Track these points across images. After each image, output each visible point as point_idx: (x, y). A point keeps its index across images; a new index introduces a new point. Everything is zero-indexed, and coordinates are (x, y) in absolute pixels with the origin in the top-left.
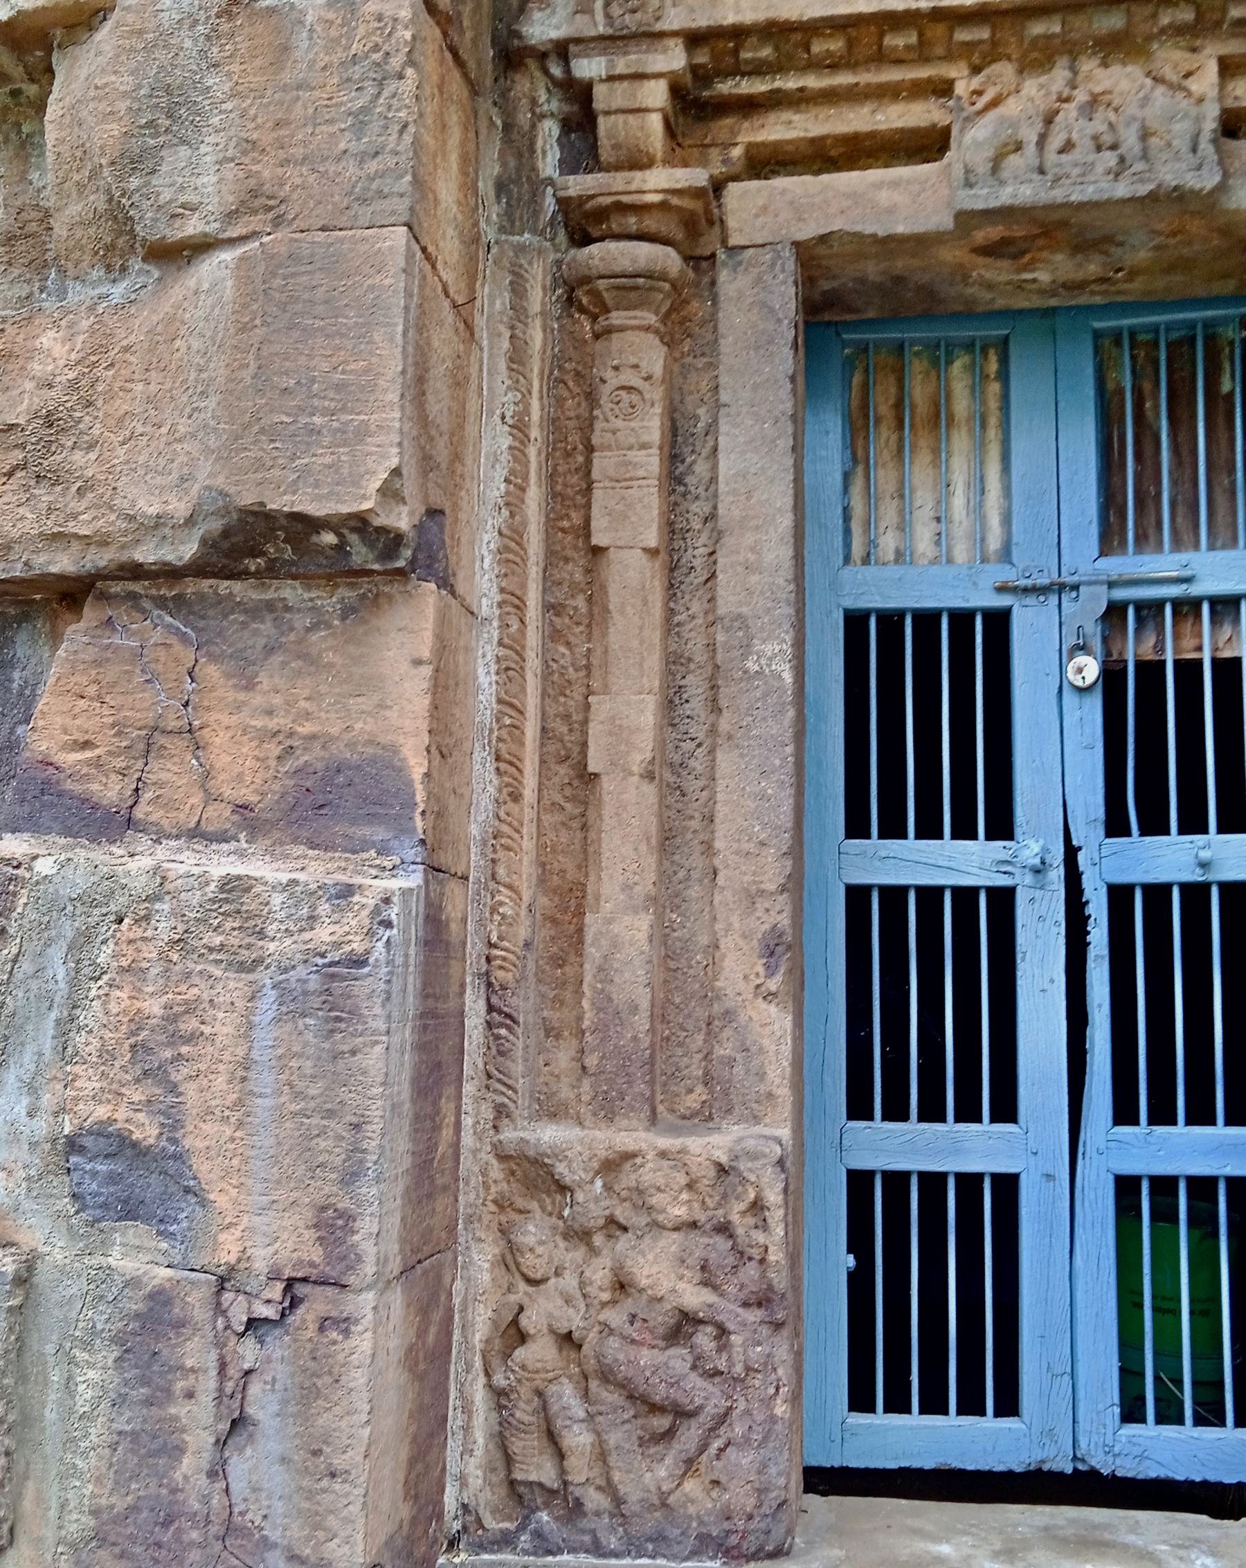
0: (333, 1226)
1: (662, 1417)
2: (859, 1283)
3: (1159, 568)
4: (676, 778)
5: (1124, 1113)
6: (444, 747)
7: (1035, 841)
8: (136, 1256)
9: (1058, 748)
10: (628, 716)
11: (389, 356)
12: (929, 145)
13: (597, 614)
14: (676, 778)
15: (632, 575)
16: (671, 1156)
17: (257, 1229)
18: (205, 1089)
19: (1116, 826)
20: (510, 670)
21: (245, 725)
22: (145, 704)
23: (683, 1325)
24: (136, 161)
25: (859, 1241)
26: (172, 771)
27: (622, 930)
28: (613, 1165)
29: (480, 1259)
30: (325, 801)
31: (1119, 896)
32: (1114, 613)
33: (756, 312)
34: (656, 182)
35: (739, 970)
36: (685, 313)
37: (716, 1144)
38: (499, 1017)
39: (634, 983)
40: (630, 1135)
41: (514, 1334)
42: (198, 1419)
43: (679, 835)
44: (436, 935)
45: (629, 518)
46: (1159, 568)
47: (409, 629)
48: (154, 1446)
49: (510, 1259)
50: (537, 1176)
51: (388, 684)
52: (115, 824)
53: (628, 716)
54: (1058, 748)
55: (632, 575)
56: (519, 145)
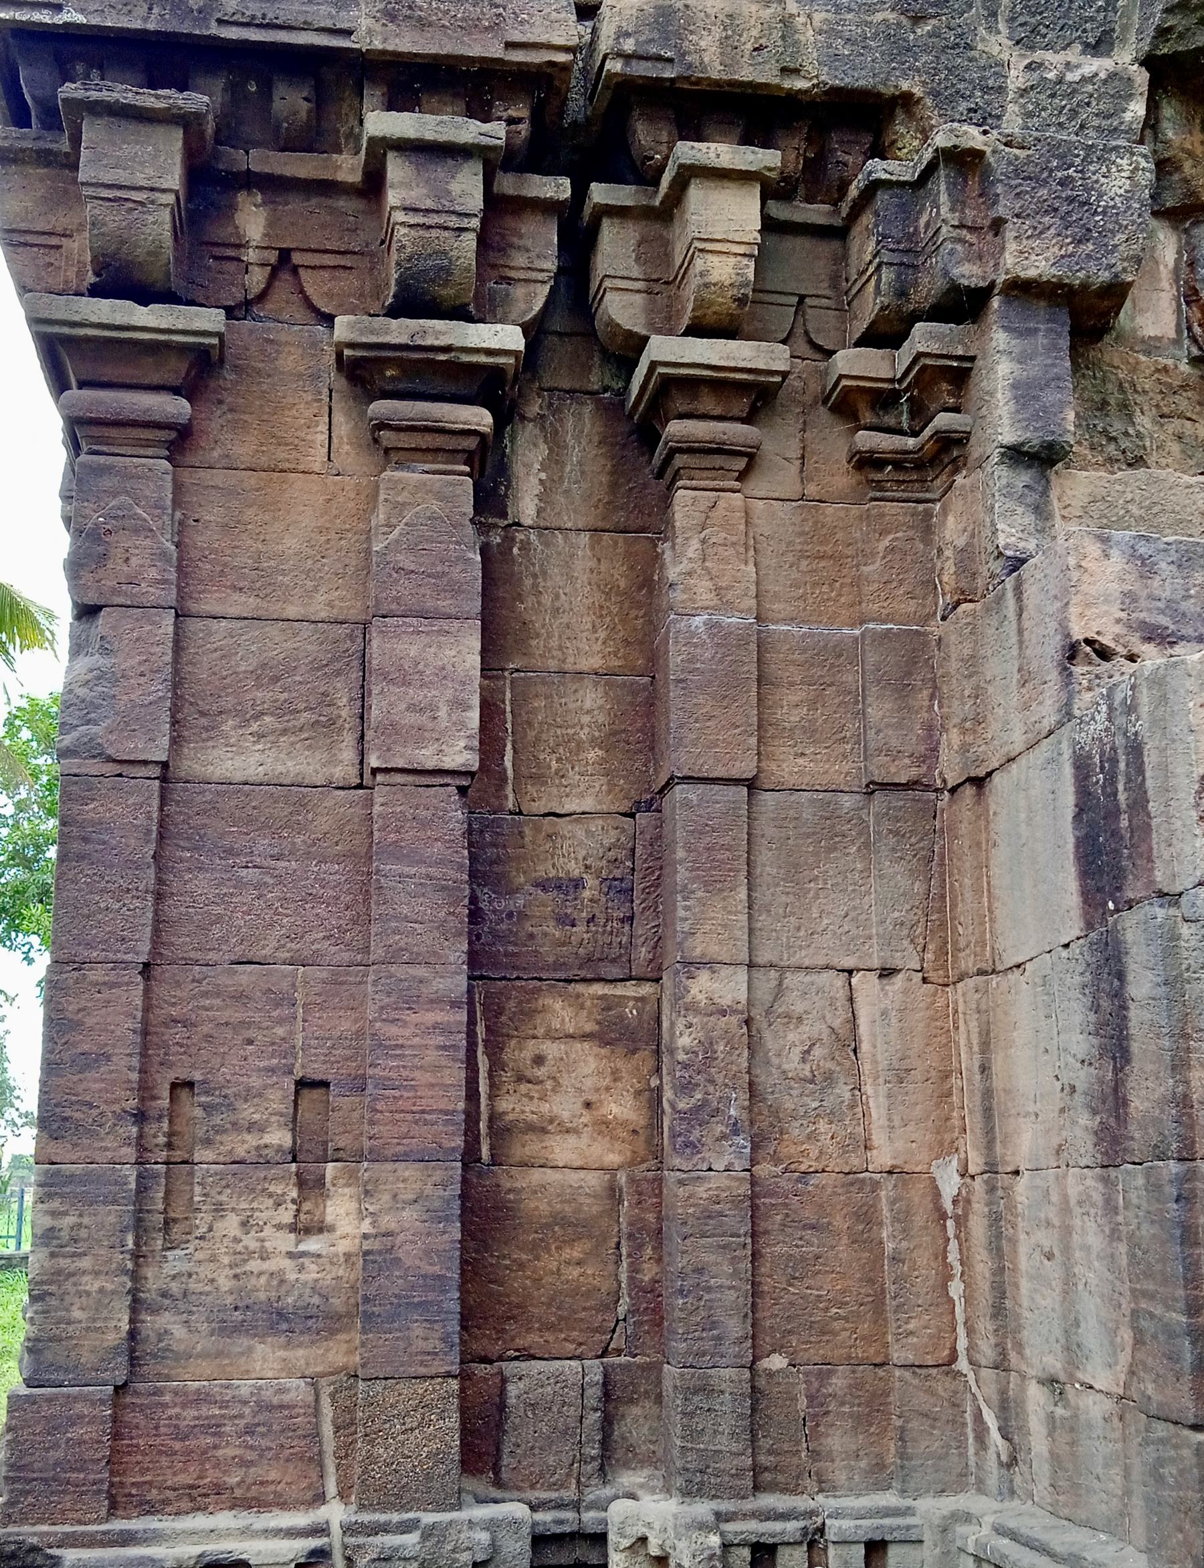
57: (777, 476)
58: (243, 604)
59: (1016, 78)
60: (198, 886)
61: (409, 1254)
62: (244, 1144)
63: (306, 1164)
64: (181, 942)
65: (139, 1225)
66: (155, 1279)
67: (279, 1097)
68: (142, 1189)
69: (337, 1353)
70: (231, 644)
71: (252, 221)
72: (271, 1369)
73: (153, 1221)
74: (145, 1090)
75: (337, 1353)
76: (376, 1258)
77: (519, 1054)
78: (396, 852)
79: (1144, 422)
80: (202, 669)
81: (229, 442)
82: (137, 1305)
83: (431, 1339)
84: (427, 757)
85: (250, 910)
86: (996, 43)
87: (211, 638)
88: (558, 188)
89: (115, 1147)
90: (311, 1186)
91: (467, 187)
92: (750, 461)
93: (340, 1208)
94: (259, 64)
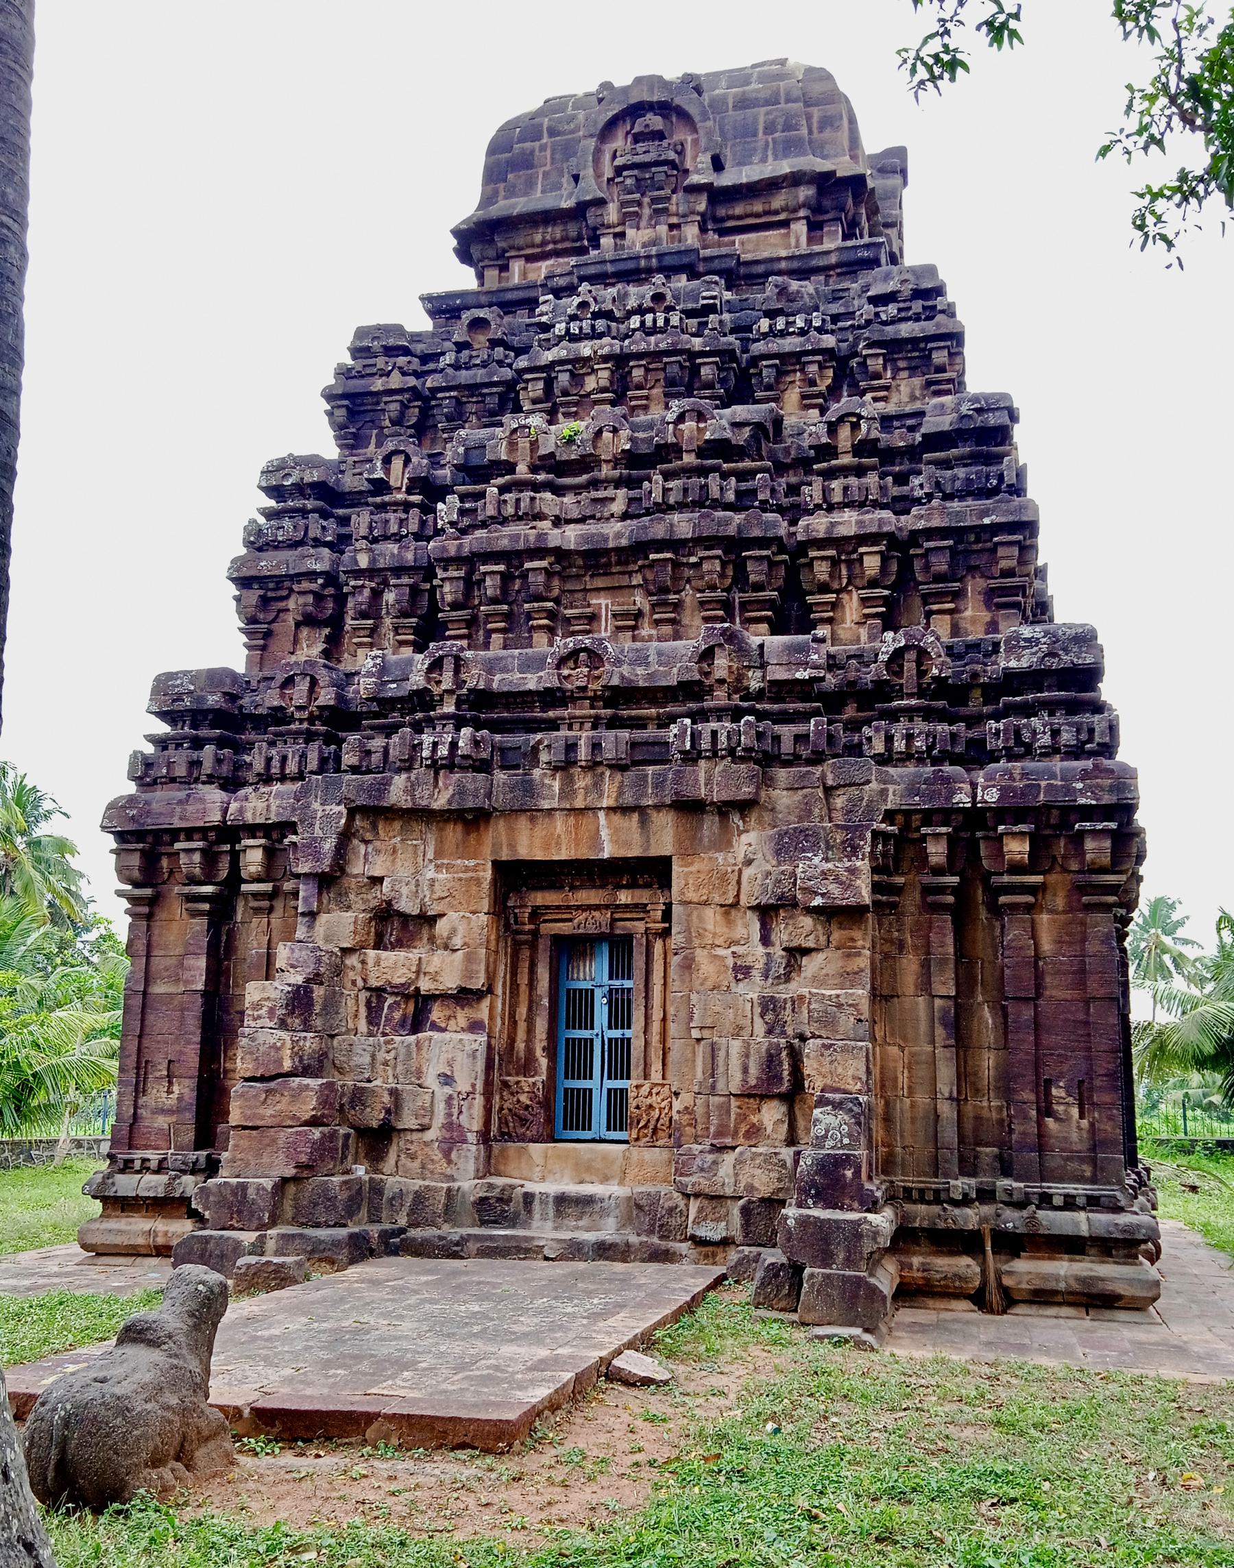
0: (473, 1086)
1: (523, 1121)
2: (565, 1108)
3: (617, 983)
4: (530, 1021)
5: (609, 1078)
6: (491, 1017)
7: (597, 1030)
8: (448, 1090)
9: (601, 1013)
10: (522, 1011)
11: (483, 967)
12: (570, 920)
13: (518, 995)
14: (530, 1021)
15: (524, 989)
16: (526, 1082)
17: (463, 1085)
18: (457, 1067)
19: (610, 1028)
20: (504, 1004)
21: (462, 1017)
22: (448, 1013)
23: (527, 1107)
24: (449, 938)
25: (566, 1100)
26: (452, 1022)
27: (520, 1046)
28: (518, 1083)
29: (497, 1098)
30: (475, 1027)
31: (610, 1040)
32: (610, 991)
33: (544, 946)
34: (527, 927)
35: (539, 1052)
36: (533, 946)
37: (531, 1080)
38: (501, 1059)
39: (522, 1054)
40: (521, 1078)
41: (501, 1109)
42: (455, 1111)
43: (530, 1031)
44: (490, 1047)
45: (523, 980)
46: (617, 983)
47: (486, 1003)
48: (450, 1115)
49: (502, 1098)
50: (505, 1084)
51: (482, 1011)
52: (444, 1030)
53: (522, 1011)
54: (601, 1013)
55: (524, 989)
56: (507, 919)
57: (278, 912)
58: (162, 953)
59: (319, 814)
60: (151, 1018)
61: (186, 1098)
62: (158, 1074)
63: (170, 1077)
64: (147, 1030)
65: (136, 1091)
66: (140, 1102)
67: (165, 1064)
68: (137, 1083)
69: (173, 1119)
70: (158, 963)
71: (165, 863)
72: (162, 1122)
73: (140, 1089)
74: (138, 1062)
75: (173, 1119)
76: (180, 1099)
77: (230, 1053)
78: (188, 1009)
79: (352, 897)
80: (153, 969)
81: (161, 915)
82: (136, 1107)
83: (190, 1116)
84: (194, 987)
85: (160, 1023)
86: (316, 806)
87: (155, 961)
88: (227, 847)
89: (133, 1074)
90: (170, 1083)
91: (197, 857)
92: (271, 910)
93: (176, 1088)
94: (157, 834)
